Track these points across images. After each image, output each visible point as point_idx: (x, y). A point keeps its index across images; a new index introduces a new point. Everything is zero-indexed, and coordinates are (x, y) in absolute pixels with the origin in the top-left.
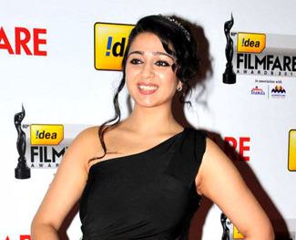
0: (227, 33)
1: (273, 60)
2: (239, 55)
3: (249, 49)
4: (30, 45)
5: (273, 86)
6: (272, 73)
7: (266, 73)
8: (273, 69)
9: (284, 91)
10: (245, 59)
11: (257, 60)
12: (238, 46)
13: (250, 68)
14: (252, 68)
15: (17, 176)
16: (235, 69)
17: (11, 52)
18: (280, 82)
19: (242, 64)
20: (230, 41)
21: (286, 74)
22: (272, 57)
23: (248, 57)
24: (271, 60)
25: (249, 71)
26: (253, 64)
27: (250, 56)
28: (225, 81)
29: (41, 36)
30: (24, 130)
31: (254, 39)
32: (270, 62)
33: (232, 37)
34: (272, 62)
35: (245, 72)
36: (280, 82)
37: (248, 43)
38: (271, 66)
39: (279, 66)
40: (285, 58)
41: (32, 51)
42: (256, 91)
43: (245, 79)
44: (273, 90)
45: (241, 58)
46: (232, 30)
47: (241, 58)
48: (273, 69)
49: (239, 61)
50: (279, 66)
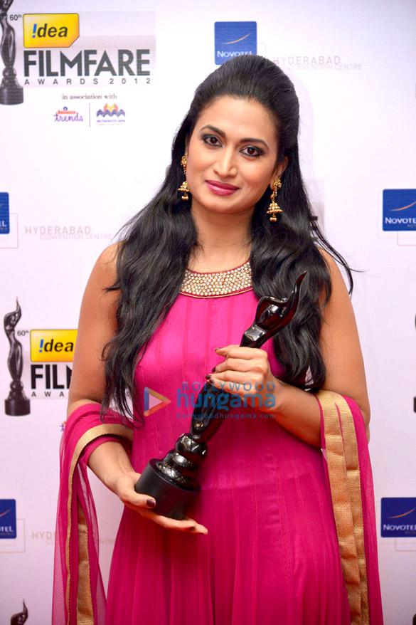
1: (97, 58)
6: (96, 82)
7: (83, 82)
8: (97, 74)
9: (122, 112)
11: (64, 60)
13: (50, 74)
14: (56, 74)
18: (114, 96)
19: (34, 70)
21: (124, 81)
22: (94, 52)
24: (92, 57)
25: (49, 80)
26: (56, 67)
27: (49, 53)
31: (57, 23)
32: (88, 63)
34: (94, 62)
35: (41, 82)
36: (114, 96)
37: (44, 31)
38: (93, 68)
39: (110, 68)
40: (121, 53)
42: (64, 115)
44: (99, 113)
48: (97, 74)
49: (28, 64)
50: (110, 68)
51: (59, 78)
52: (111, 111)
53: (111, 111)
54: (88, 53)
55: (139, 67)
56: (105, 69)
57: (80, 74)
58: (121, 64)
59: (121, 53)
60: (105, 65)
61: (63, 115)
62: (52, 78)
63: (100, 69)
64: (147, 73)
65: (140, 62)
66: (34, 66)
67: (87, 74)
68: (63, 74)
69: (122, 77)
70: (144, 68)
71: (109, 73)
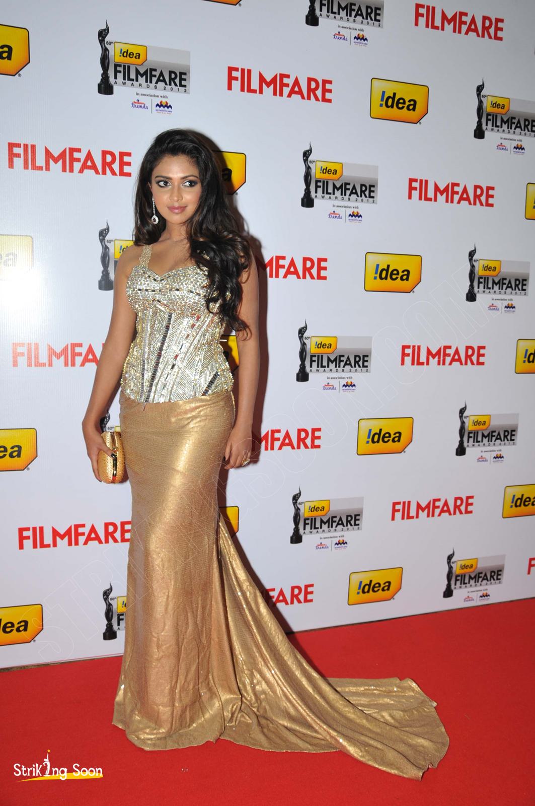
0: (305, 161)
1: (350, 187)
2: (317, 181)
3: (327, 176)
4: (116, 166)
5: (350, 211)
10: (324, 186)
12: (316, 173)
13: (328, 193)
14: (330, 194)
15: (100, 288)
16: (313, 194)
17: (97, 172)
18: (357, 208)
19: (320, 190)
20: (308, 168)
23: (326, 184)
25: (327, 196)
26: (330, 190)
27: (327, 182)
28: (303, 205)
29: (126, 159)
30: (108, 245)
32: (346, 189)
33: (310, 165)
35: (323, 197)
36: (357, 208)
37: (326, 171)
38: (348, 192)
39: (356, 193)
41: (117, 170)
43: (322, 204)
45: (319, 184)
46: (310, 158)
47: (319, 184)
49: (317, 187)
51: (332, 196)
52: (355, 215)
53: (355, 215)
54: (347, 184)
55: (370, 194)
56: (354, 193)
57: (342, 195)
58: (362, 191)
59: (362, 185)
60: (354, 191)
61: (333, 215)
62: (329, 196)
63: (351, 193)
64: (373, 197)
65: (370, 191)
66: (120, 74)
67: (345, 195)
68: (334, 194)
69: (361, 198)
70: (372, 194)
71: (356, 195)
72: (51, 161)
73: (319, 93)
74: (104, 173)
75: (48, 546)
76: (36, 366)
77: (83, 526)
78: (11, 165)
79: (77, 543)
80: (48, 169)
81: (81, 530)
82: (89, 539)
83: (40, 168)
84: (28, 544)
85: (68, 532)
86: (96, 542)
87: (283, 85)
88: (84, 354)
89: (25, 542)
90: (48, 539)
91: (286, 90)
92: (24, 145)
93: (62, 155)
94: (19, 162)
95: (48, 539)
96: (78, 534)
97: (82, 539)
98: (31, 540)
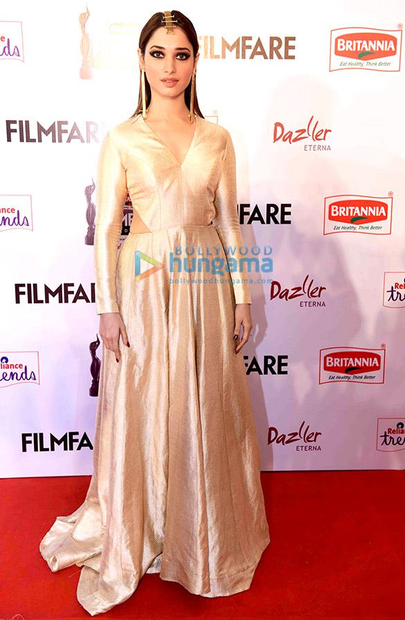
72: (43, 134)
73: (282, 51)
74: (88, 141)
75: (47, 450)
76: (35, 302)
77: (77, 433)
78: (9, 140)
79: (71, 449)
80: (40, 140)
81: (75, 437)
82: (81, 445)
83: (34, 141)
84: (30, 447)
85: (64, 438)
86: (88, 447)
87: (246, 47)
88: (75, 293)
89: (27, 445)
90: (47, 444)
91: (249, 52)
92: (20, 121)
93: (52, 128)
94: (15, 136)
95: (47, 444)
96: (72, 441)
97: (76, 445)
98: (32, 445)
